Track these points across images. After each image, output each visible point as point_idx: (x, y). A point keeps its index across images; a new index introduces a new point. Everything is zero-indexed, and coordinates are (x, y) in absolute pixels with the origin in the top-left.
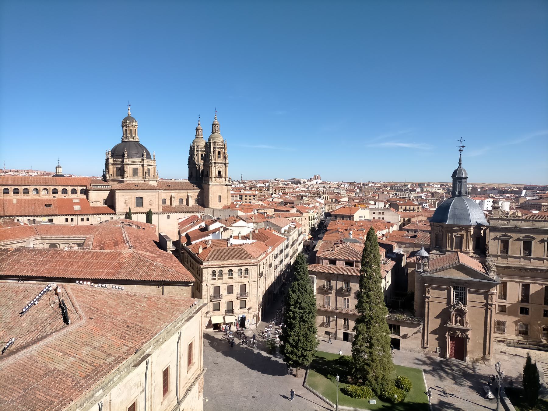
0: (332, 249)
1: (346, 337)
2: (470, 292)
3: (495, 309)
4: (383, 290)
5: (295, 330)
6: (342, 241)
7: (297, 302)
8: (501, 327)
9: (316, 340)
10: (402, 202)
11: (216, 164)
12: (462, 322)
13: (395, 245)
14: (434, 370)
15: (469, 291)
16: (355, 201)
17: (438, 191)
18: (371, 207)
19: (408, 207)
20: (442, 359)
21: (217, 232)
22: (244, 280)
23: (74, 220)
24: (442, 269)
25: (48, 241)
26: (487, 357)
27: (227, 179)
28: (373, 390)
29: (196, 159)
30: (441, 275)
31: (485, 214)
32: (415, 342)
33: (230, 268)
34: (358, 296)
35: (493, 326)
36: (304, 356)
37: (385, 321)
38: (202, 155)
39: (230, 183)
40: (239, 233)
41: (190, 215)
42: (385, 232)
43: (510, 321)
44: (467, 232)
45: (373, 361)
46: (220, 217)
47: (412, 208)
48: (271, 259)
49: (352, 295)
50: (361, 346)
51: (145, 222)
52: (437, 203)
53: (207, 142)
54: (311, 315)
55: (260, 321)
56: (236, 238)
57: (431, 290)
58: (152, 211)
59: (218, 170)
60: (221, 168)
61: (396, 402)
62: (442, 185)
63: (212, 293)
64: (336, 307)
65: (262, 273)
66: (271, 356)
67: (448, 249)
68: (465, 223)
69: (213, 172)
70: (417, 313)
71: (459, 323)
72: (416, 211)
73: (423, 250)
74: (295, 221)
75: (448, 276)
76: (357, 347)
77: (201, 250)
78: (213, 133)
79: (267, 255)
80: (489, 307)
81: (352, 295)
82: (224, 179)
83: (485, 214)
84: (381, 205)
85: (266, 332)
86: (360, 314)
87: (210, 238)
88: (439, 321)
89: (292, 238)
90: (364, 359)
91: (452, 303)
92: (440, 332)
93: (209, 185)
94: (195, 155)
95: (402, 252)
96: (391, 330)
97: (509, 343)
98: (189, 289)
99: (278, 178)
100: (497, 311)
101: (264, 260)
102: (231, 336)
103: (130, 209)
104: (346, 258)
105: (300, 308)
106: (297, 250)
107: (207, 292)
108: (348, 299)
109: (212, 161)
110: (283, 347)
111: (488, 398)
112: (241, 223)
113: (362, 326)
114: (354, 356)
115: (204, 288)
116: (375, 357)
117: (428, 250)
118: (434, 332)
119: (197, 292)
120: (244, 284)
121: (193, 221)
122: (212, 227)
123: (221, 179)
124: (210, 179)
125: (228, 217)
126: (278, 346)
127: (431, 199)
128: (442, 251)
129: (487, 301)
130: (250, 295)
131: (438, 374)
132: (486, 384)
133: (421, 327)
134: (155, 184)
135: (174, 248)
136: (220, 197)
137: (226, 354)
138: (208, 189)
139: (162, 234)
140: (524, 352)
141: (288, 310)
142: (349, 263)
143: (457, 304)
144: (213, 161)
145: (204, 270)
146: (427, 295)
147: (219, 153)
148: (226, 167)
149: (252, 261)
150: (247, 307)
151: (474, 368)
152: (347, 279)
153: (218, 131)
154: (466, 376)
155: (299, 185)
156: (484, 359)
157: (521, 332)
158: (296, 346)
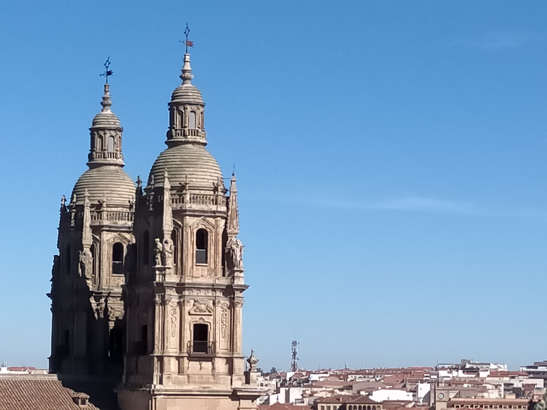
11: (186, 293)
27: (240, 365)
29: (89, 268)
38: (117, 248)
39: (252, 386)
53: (144, 185)
59: (197, 320)
60: (210, 312)
78: (172, 144)
82: (221, 365)
93: (151, 395)
94: (87, 250)
99: (475, 359)
109: (168, 279)
123: (207, 365)
124: (156, 365)
144: (172, 278)
148: (232, 306)
153: (195, 133)
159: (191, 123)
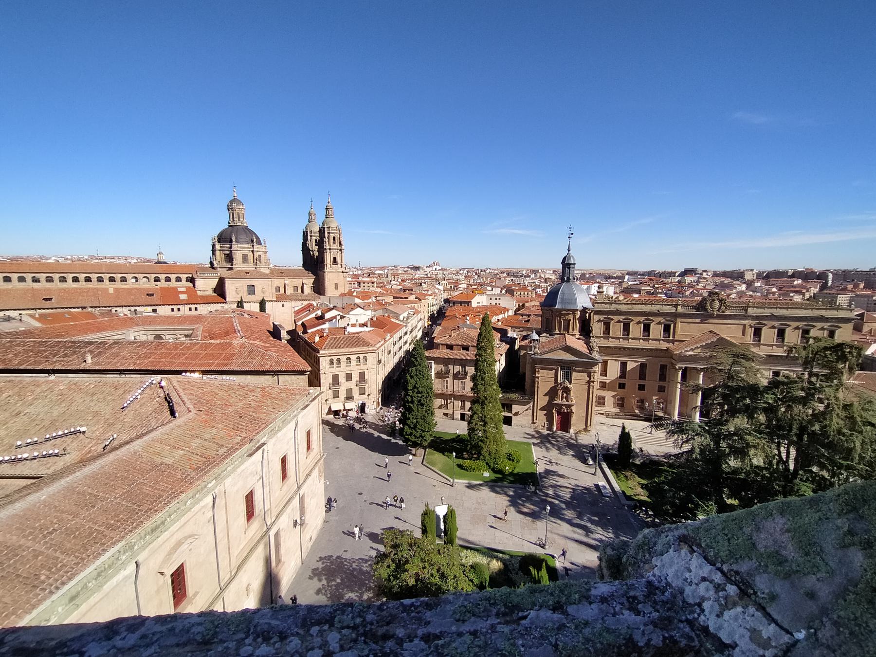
0: (450, 334)
1: (463, 417)
2: (575, 371)
3: (597, 385)
4: (497, 373)
5: (414, 413)
6: (458, 327)
7: (415, 387)
8: (601, 401)
9: (434, 422)
10: (517, 288)
12: (567, 399)
13: (509, 329)
14: (542, 442)
15: (574, 369)
16: (473, 287)
17: (551, 277)
18: (488, 293)
19: (522, 293)
20: (549, 432)
21: (334, 320)
22: (362, 368)
23: (181, 309)
24: (550, 351)
25: (151, 332)
26: (588, 428)
28: (487, 464)
29: (310, 246)
30: (550, 356)
31: (590, 298)
32: (526, 418)
33: (348, 356)
34: (474, 378)
35: (594, 400)
36: (423, 437)
37: (498, 401)
38: (316, 240)
40: (357, 320)
41: (306, 303)
42: (500, 317)
43: (609, 395)
44: (574, 316)
45: (487, 438)
46: (336, 305)
47: (526, 293)
48: (389, 345)
49: (468, 378)
50: (476, 424)
51: (258, 310)
52: (549, 288)
54: (428, 399)
55: (380, 406)
56: (354, 325)
57: (540, 371)
58: (265, 299)
60: (337, 255)
61: (507, 473)
62: (554, 271)
63: (331, 381)
64: (453, 390)
65: (381, 360)
66: (391, 438)
67: (557, 331)
68: (572, 308)
69: (328, 259)
70: (528, 392)
71: (564, 399)
72: (529, 297)
73: (534, 333)
74: (414, 308)
75: (556, 357)
76: (473, 425)
77: (317, 339)
79: (385, 342)
80: (591, 383)
81: (468, 378)
82: (340, 266)
83: (590, 298)
84: (497, 291)
85: (386, 416)
86: (476, 395)
87: (326, 326)
88: (547, 398)
89: (411, 325)
90: (479, 436)
91: (559, 381)
92: (548, 409)
93: (324, 272)
95: (515, 336)
96: (504, 408)
97: (608, 415)
98: (305, 378)
100: (598, 387)
101: (383, 347)
102: (351, 422)
103: (241, 297)
104: (463, 343)
105: (418, 392)
106: (416, 336)
107: (326, 379)
108: (465, 382)
110: (402, 430)
111: (588, 464)
112: (358, 311)
113: (477, 407)
114: (469, 434)
115: (322, 377)
116: (488, 434)
117: (539, 334)
118: (542, 409)
119: (315, 380)
120: (363, 371)
121: (309, 308)
122: (328, 316)
123: (336, 266)
125: (345, 305)
126: (397, 428)
127: (544, 285)
128: (552, 334)
129: (590, 379)
130: (369, 381)
131: (545, 445)
132: (586, 453)
133: (531, 404)
134: (267, 271)
135: (289, 337)
136: (336, 284)
137: (346, 438)
138: (324, 276)
139: (276, 323)
140: (619, 422)
141: (407, 394)
142: (466, 348)
143: (564, 382)
144: (328, 247)
145: (321, 358)
146: (537, 375)
147: (334, 238)
149: (371, 349)
150: (367, 394)
151: (577, 439)
152: (463, 363)
154: (570, 446)
155: (418, 272)
156: (586, 430)
157: (618, 405)
158: (415, 428)
159: (330, 213)
